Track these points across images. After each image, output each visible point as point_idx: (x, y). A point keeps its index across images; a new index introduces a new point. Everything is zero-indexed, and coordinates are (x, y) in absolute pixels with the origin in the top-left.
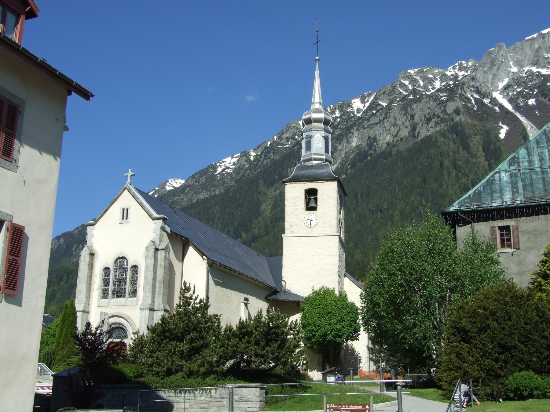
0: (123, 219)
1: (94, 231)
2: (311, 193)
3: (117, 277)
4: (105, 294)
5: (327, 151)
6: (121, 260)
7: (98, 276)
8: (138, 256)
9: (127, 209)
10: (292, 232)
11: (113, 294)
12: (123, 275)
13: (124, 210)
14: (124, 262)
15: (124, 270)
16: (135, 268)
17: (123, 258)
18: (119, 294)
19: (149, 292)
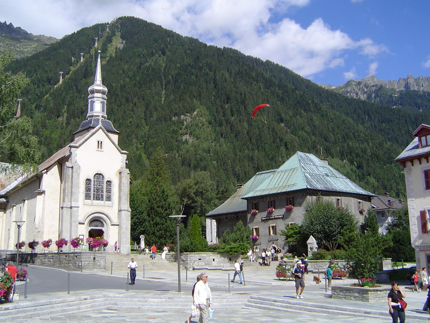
1: (76, 152)
3: (95, 186)
4: (87, 197)
5: (103, 111)
6: (99, 175)
9: (101, 142)
11: (94, 197)
12: (100, 186)
13: (98, 142)
14: (100, 177)
15: (100, 183)
16: (109, 182)
17: (100, 174)
18: (98, 197)
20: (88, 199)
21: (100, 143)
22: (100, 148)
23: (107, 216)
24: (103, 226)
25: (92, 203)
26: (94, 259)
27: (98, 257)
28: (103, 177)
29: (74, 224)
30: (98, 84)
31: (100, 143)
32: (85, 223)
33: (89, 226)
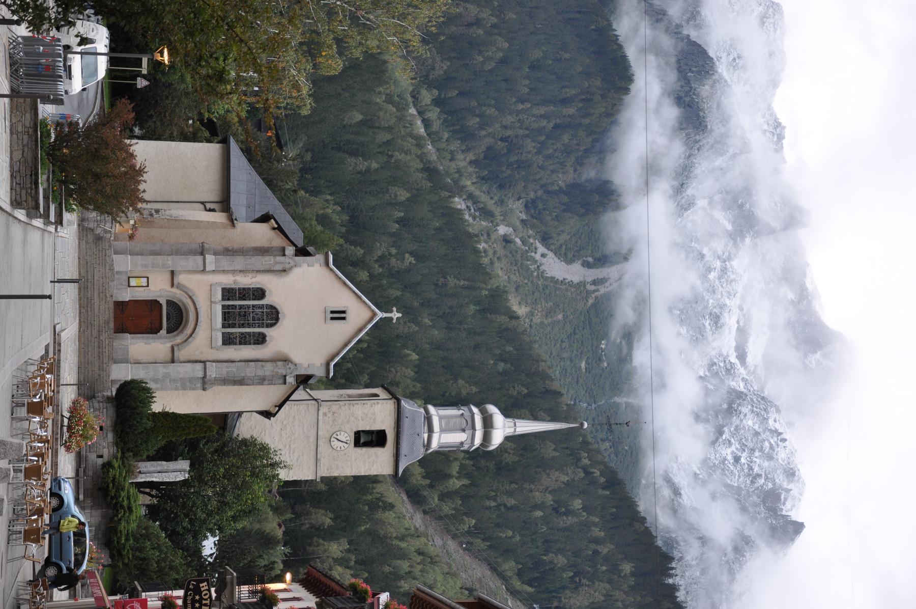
1: (317, 266)
2: (376, 439)
4: (228, 293)
6: (273, 316)
7: (254, 280)
8: (279, 339)
9: (344, 318)
10: (325, 414)
12: (254, 320)
13: (344, 312)
17: (277, 319)
18: (229, 317)
19: (228, 373)
20: (223, 296)
21: (343, 315)
23: (191, 335)
24: (169, 331)
25: (215, 303)
28: (272, 325)
29: (169, 261)
30: (503, 428)
31: (343, 315)
32: (174, 290)
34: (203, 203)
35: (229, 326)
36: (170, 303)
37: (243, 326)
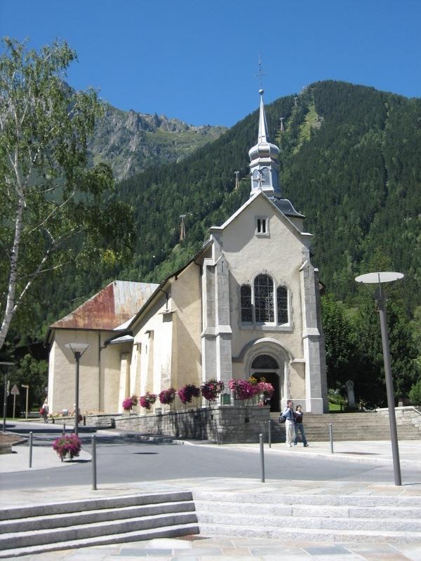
0: (259, 231)
6: (264, 281)
13: (259, 221)
21: (262, 221)
22: (262, 231)
26: (247, 420)
27: (253, 417)
30: (263, 144)
31: (262, 221)
33: (253, 367)
34: (100, 349)
35: (272, 316)
36: (254, 366)
37: (272, 305)
